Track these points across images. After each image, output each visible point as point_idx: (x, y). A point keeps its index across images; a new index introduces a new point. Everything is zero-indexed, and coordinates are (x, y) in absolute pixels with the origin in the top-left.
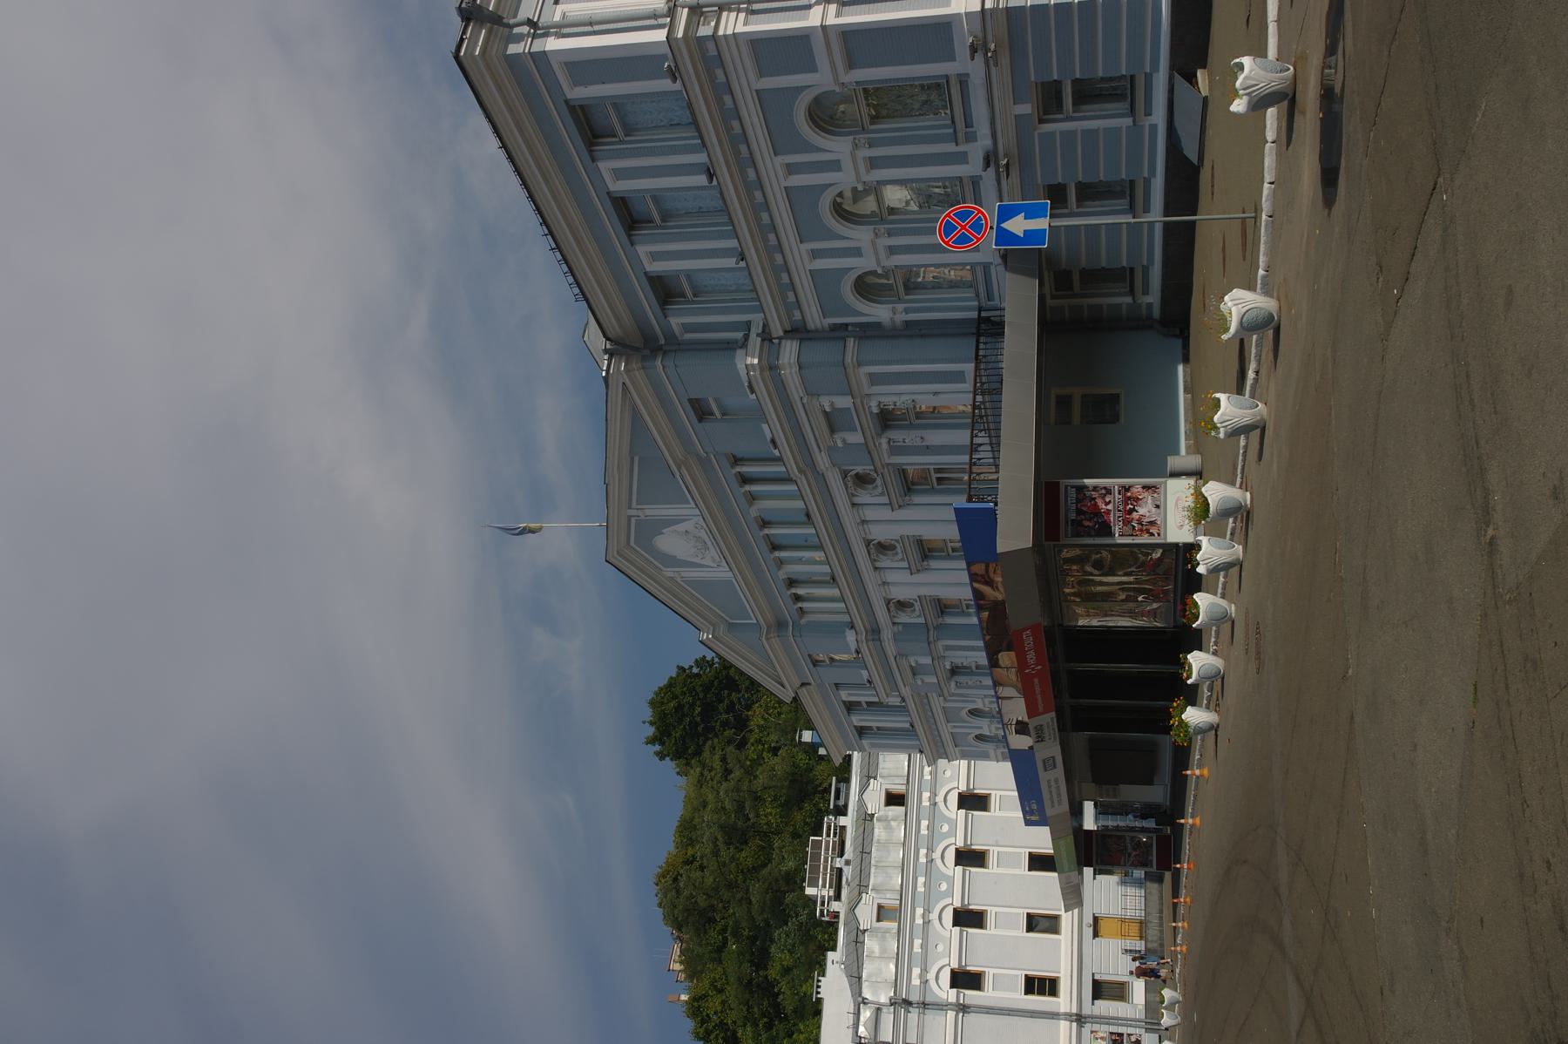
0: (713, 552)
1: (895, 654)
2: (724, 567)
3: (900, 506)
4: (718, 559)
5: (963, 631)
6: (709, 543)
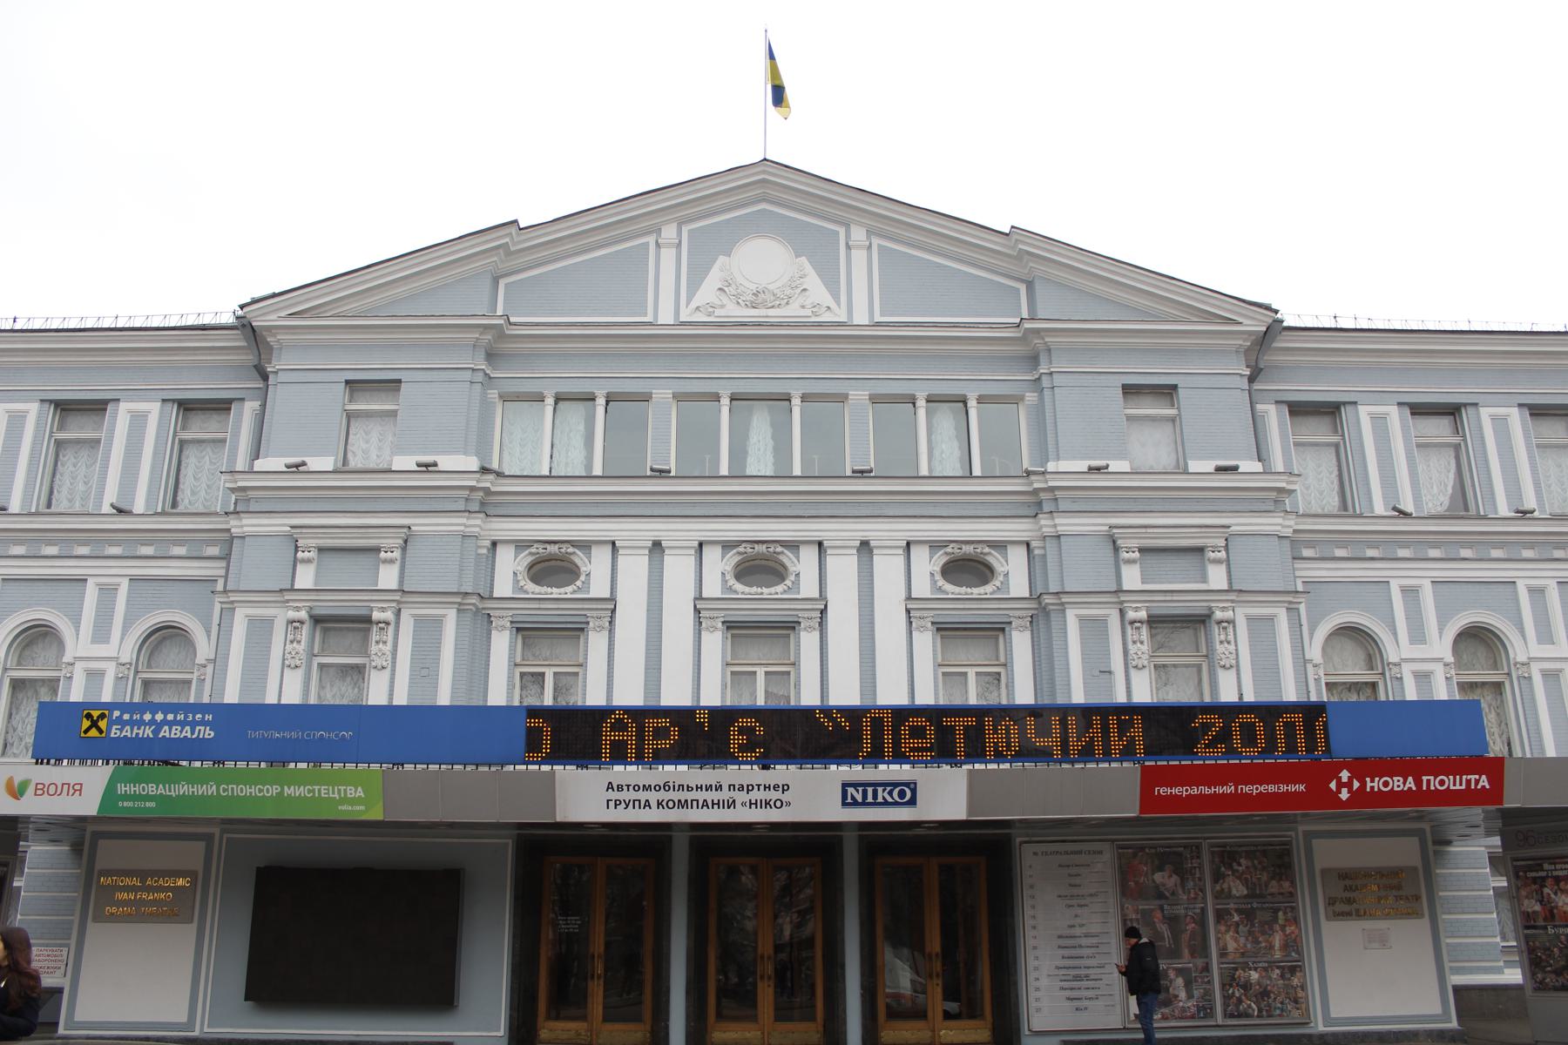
0: (734, 311)
1: (413, 528)
2: (690, 315)
3: (908, 611)
4: (718, 312)
5: (475, 662)
6: (763, 312)
